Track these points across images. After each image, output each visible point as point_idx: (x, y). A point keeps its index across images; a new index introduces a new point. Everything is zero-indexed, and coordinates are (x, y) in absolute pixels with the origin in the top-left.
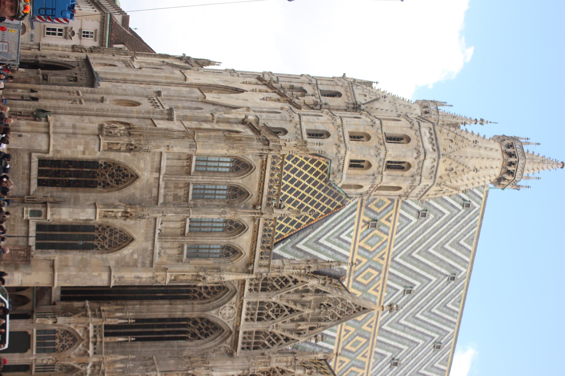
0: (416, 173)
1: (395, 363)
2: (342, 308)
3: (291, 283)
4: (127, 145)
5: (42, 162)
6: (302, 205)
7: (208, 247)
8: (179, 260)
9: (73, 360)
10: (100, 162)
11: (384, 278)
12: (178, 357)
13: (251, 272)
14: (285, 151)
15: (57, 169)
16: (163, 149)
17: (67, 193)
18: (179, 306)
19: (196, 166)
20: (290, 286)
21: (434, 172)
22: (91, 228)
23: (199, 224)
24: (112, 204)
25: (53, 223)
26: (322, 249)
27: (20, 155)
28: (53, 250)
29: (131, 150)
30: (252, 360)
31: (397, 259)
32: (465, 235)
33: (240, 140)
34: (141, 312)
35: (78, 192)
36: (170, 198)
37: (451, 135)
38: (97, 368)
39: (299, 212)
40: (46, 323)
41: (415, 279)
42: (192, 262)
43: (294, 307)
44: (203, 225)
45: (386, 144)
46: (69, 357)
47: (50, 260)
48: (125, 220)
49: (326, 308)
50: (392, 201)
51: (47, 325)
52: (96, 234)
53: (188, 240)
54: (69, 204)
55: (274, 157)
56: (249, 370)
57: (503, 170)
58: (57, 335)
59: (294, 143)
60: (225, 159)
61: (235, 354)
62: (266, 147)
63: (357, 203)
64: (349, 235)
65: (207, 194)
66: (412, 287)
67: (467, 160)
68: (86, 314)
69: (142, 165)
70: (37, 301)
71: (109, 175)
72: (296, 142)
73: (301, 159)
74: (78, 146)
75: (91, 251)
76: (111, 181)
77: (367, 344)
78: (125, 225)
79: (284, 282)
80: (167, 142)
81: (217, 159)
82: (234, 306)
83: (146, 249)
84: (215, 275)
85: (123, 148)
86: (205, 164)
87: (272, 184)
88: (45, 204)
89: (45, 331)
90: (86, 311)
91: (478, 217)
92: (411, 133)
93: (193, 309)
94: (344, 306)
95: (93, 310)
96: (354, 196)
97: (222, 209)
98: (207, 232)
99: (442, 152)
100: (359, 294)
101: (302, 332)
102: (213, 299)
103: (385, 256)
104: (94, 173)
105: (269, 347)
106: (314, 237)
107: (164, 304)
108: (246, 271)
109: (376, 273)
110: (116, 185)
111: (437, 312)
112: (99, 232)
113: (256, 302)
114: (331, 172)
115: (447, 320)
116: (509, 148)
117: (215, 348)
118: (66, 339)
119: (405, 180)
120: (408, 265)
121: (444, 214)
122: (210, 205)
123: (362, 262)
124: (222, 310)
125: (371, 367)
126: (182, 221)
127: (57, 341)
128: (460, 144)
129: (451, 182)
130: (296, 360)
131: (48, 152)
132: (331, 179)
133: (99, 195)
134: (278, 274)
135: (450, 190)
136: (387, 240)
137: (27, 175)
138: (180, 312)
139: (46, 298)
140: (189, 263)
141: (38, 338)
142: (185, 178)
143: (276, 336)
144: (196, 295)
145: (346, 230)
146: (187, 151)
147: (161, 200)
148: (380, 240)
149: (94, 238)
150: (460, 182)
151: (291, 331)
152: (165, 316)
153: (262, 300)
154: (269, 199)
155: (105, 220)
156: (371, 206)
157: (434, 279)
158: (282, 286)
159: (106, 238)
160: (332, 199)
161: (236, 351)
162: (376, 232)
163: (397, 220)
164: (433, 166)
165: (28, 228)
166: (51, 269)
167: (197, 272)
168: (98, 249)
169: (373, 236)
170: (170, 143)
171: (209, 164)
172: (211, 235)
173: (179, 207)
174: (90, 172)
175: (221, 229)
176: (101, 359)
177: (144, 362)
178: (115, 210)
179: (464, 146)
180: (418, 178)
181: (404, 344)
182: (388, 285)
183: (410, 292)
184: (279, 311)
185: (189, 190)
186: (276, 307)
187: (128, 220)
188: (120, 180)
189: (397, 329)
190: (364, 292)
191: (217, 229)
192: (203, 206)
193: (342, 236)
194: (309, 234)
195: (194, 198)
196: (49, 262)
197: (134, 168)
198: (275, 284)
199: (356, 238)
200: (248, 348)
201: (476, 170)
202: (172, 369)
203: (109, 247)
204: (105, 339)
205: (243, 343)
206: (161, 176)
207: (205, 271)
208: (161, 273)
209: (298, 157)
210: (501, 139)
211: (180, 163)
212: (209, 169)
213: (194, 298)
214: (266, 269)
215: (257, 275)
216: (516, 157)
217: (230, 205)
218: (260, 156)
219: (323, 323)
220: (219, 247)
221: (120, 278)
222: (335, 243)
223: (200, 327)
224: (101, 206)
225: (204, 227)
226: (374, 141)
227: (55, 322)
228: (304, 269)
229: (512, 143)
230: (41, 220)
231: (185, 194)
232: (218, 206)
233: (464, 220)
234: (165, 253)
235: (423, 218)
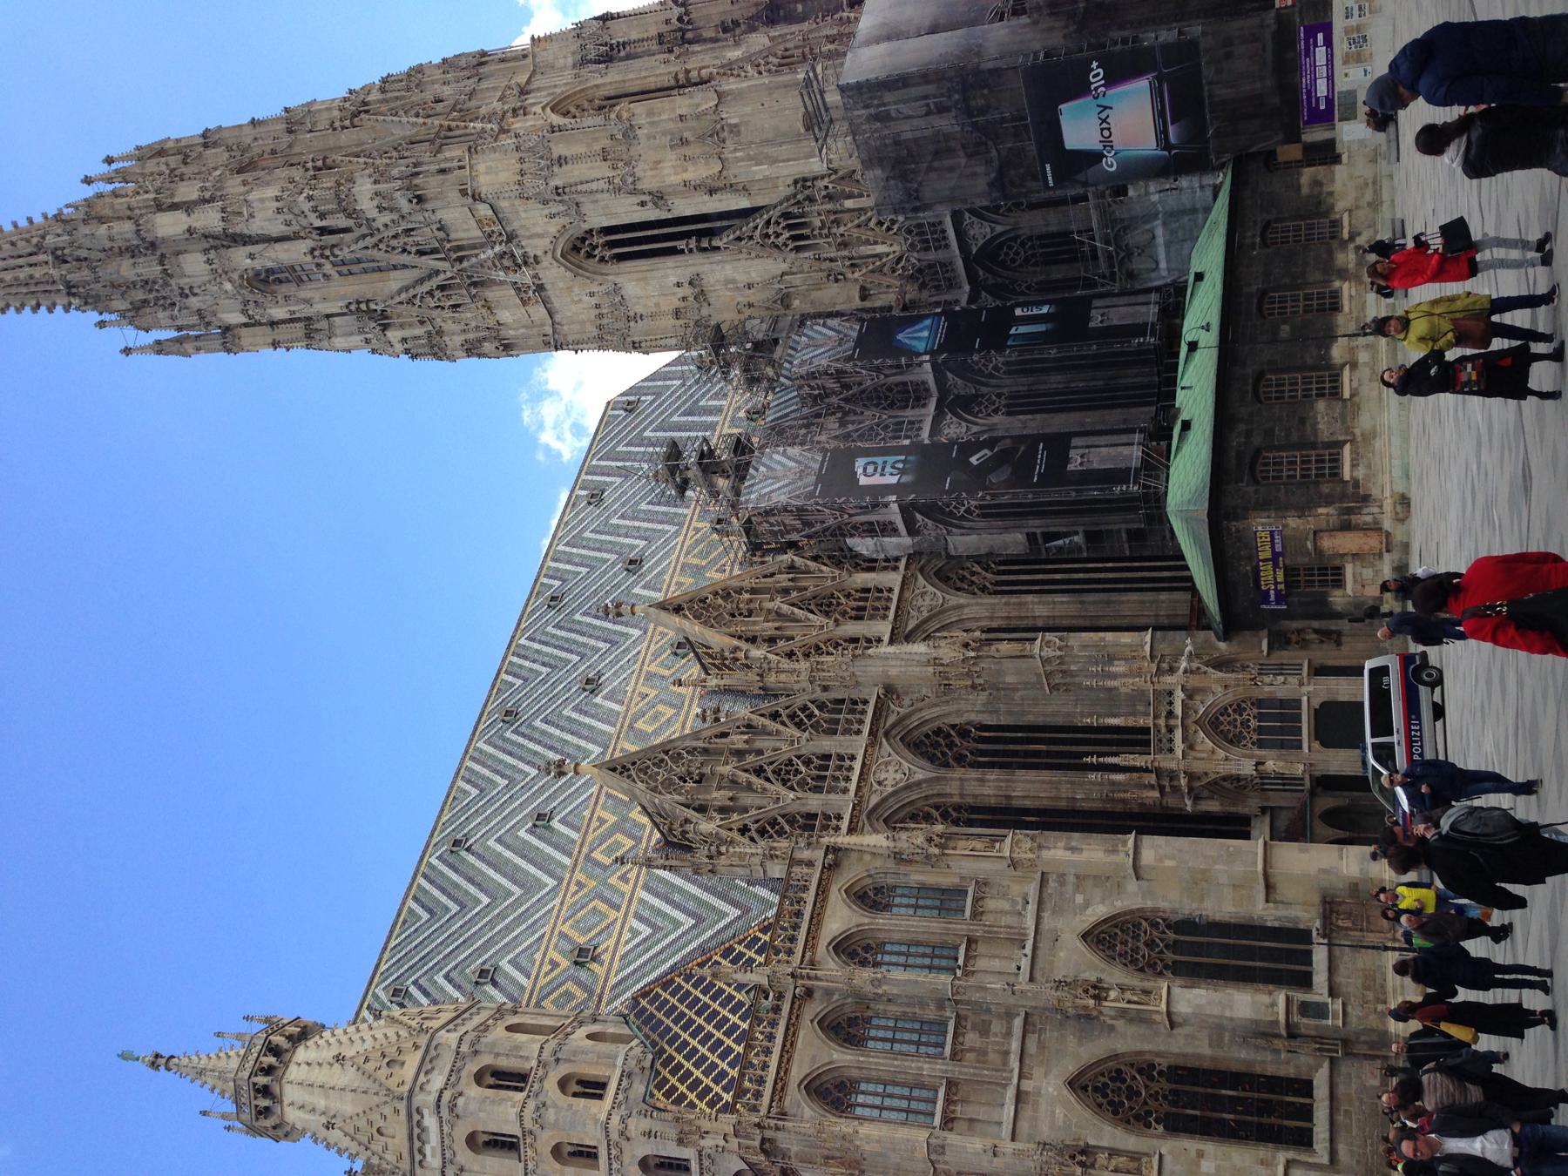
0: (466, 1060)
1: (592, 685)
2: (658, 774)
3: (753, 827)
4: (1092, 1166)
5: (1303, 1140)
6: (714, 998)
7: (919, 912)
8: (982, 884)
9: (1217, 681)
10: (1161, 1128)
11: (582, 845)
12: (998, 689)
13: (833, 850)
14: (727, 1122)
15: (1265, 1120)
16: (1008, 1147)
17: (1240, 1056)
18: (991, 792)
19: (934, 1102)
20: (757, 822)
21: (427, 1063)
22: (1178, 970)
23: (936, 962)
24: (1131, 1021)
25: (1271, 987)
26: (691, 905)
27: (1358, 1162)
28: (1269, 924)
29: (1083, 1152)
30: (846, 674)
31: (551, 882)
32: (416, 930)
33: (827, 1158)
34: (1072, 783)
35: (1213, 1059)
36: (997, 1027)
37: (377, 1147)
38: (1165, 666)
39: (714, 975)
40: (1281, 764)
41: (526, 842)
42: (957, 880)
43: (753, 779)
44: (927, 961)
45: (520, 1135)
46: (1226, 687)
47: (1275, 902)
48: (1100, 980)
49: (690, 773)
50: (538, 1004)
51: (1279, 758)
52: (1170, 956)
53: (961, 926)
54: (1234, 1029)
55: (754, 1109)
56: (854, 656)
57: (288, 1056)
58: (1255, 737)
59: (708, 1143)
60: (867, 1112)
61: (881, 691)
62: (769, 1134)
63: (607, 1005)
64: (635, 933)
65: (912, 1031)
66: (535, 826)
67: (356, 1085)
68: (1189, 781)
69: (1059, 1112)
70: (1302, 817)
71: (1139, 1094)
72: (702, 1143)
73: (702, 1105)
74: (1213, 1171)
75: (1180, 917)
76: (1134, 1078)
77: (635, 719)
78: (1103, 971)
79: (768, 828)
80: (998, 1163)
81: (885, 1114)
82: (876, 786)
83: (1054, 912)
84: (905, 845)
85: (1102, 1158)
86: (914, 1105)
87: (765, 1043)
88: (1292, 1033)
89: (1282, 745)
90: (1191, 789)
91: (383, 968)
92: (464, 1155)
93: (962, 785)
94: (653, 777)
95: (1176, 789)
96: (611, 1017)
97: (880, 991)
98: (918, 944)
99: (402, 1106)
100: (636, 815)
101: (743, 729)
102: (919, 804)
103: (573, 888)
104: (1174, 1104)
105: (813, 702)
106: (704, 931)
107: (1024, 797)
108: (840, 854)
109: (597, 855)
110: (1123, 1068)
111: (498, 779)
112: (1162, 961)
113: (828, 792)
114: (647, 1072)
115: (484, 765)
116: (267, 1109)
117: (920, 705)
118: (1235, 727)
119: (494, 1044)
120: (532, 870)
121: (447, 977)
122: (908, 1005)
123: (619, 878)
124: (901, 780)
125: (635, 675)
126: (973, 972)
127: (1253, 723)
128: (362, 1123)
129: (399, 1036)
130: (761, 676)
131: (1289, 1164)
132: (650, 1057)
133: (1162, 1048)
134: (775, 844)
135: (405, 1019)
136: (564, 923)
137: (1339, 1110)
138: (989, 781)
139: (1283, 822)
140: (962, 878)
141: (1299, 731)
142: (960, 1073)
143: (796, 724)
144: (954, 814)
145: (638, 945)
146: (952, 1138)
147: (1018, 1023)
148: (578, 922)
149: (1175, 947)
150: (379, 1035)
151: (765, 732)
152: (1020, 773)
153: (817, 796)
154: (777, 1009)
155: (1148, 985)
156: (580, 995)
157: (491, 843)
158: (774, 823)
159: (1146, 945)
160: (655, 1012)
161: (878, 697)
162: (582, 940)
163: (538, 963)
164: (427, 1073)
165: (1330, 980)
166: (1272, 880)
167: (944, 854)
168: (1164, 920)
169: (590, 930)
170: (991, 1162)
171: (904, 1104)
172: (910, 937)
173: (976, 1003)
174: (1184, 1107)
175: (888, 948)
176: (1155, 680)
177: (1068, 680)
178: (1124, 1005)
179: (355, 1118)
180: (464, 1048)
181: (569, 719)
182: (578, 830)
183: (540, 817)
184: (784, 773)
185: (954, 1043)
186: (789, 780)
187: (1093, 979)
188: (1110, 1079)
189: (579, 747)
190: (624, 819)
191: (896, 948)
192: (922, 1004)
193: (649, 931)
194: (712, 937)
195: (943, 1024)
196: (1278, 898)
197: (1078, 1107)
198: (787, 828)
199: (622, 927)
200: (855, 702)
201: (339, 1059)
202: (1007, 664)
203: (1140, 924)
204: (1150, 722)
205: (864, 712)
206: (1015, 1081)
207: (928, 857)
208: (1023, 856)
209: (708, 1111)
210: (282, 1132)
211: (971, 1111)
212: (906, 1092)
213: (958, 808)
214: (800, 855)
215: (818, 843)
216: (255, 1084)
217: (862, 1000)
218: (785, 1114)
219: (700, 744)
220: (895, 910)
221: (1114, 851)
222: (665, 915)
223: (951, 749)
224: (1157, 1018)
225: (924, 955)
226: (546, 1141)
227: (1258, 764)
228: (720, 853)
229: (257, 1119)
230: (1300, 996)
231: (964, 1034)
232: (890, 1000)
233: (411, 963)
234: (1014, 903)
235: (486, 967)
